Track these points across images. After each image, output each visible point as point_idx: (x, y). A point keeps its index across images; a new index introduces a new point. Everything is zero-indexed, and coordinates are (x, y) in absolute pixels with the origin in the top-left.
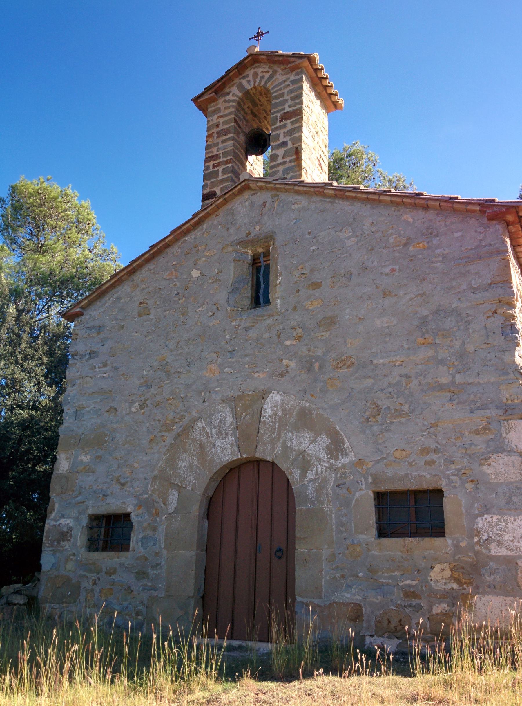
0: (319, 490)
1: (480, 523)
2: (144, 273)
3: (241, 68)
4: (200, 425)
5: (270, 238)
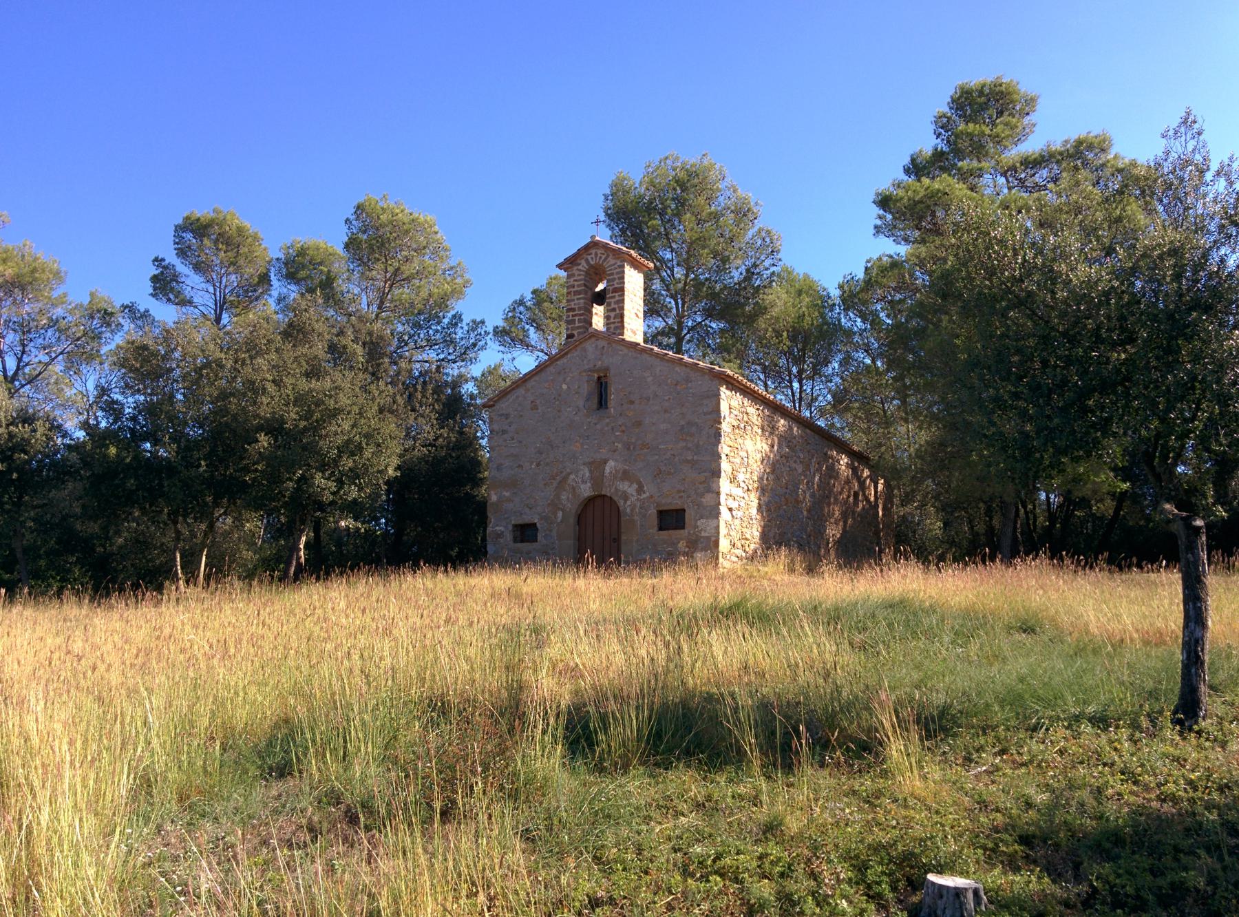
0: (632, 510)
1: (699, 523)
2: (532, 383)
3: (586, 248)
4: (572, 476)
5: (607, 369)
